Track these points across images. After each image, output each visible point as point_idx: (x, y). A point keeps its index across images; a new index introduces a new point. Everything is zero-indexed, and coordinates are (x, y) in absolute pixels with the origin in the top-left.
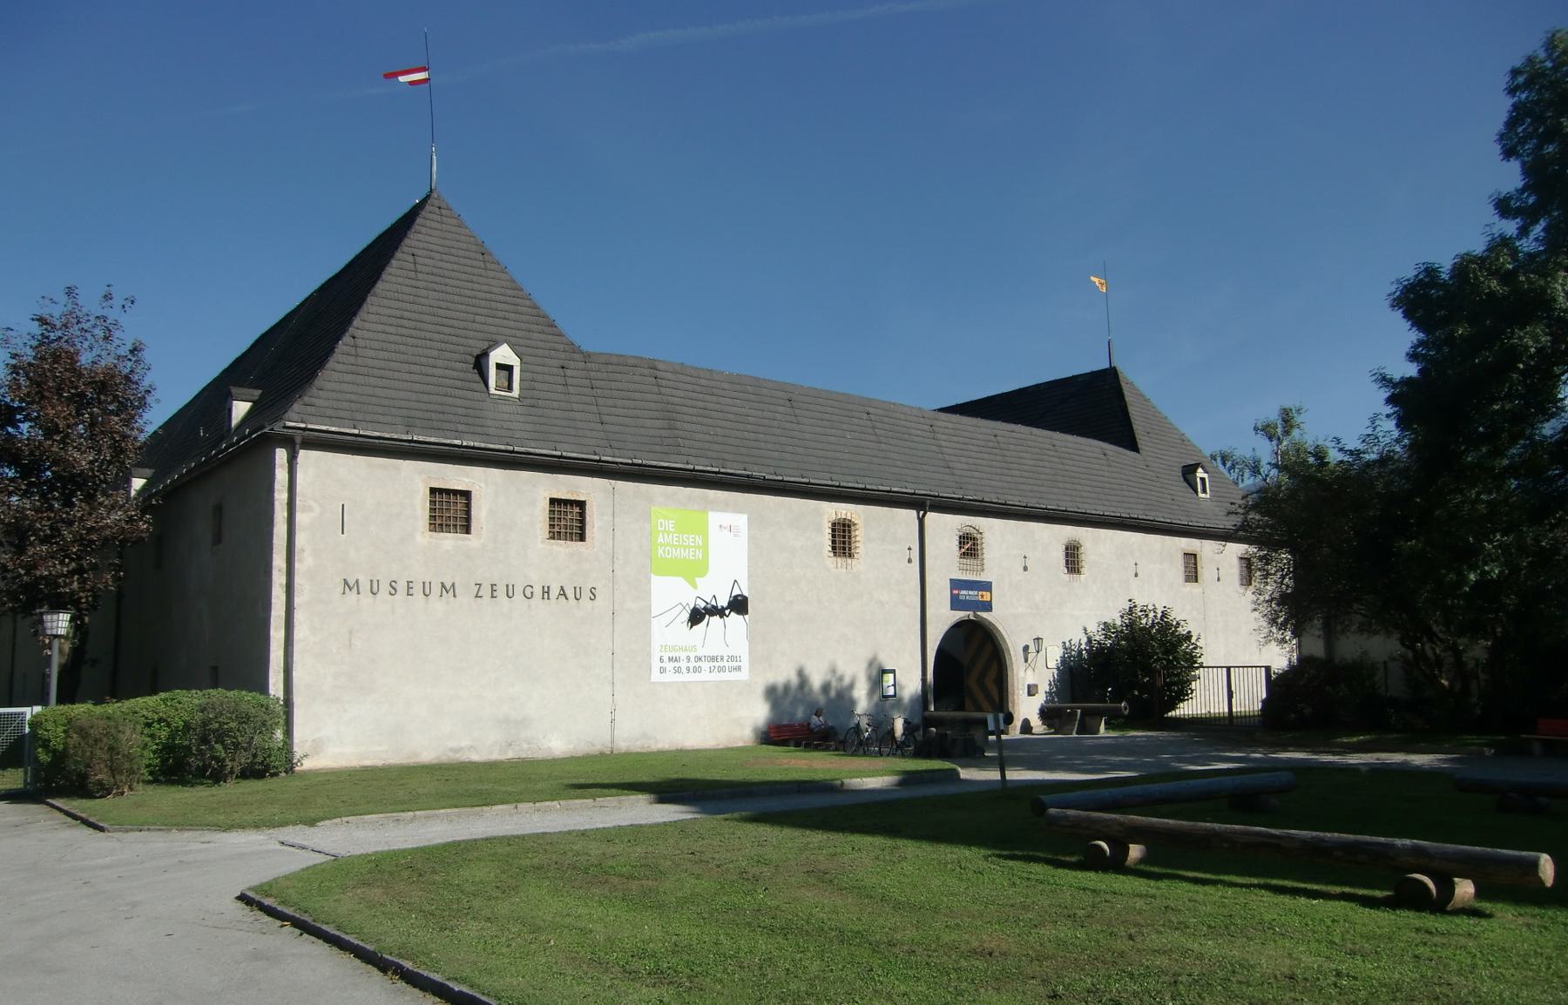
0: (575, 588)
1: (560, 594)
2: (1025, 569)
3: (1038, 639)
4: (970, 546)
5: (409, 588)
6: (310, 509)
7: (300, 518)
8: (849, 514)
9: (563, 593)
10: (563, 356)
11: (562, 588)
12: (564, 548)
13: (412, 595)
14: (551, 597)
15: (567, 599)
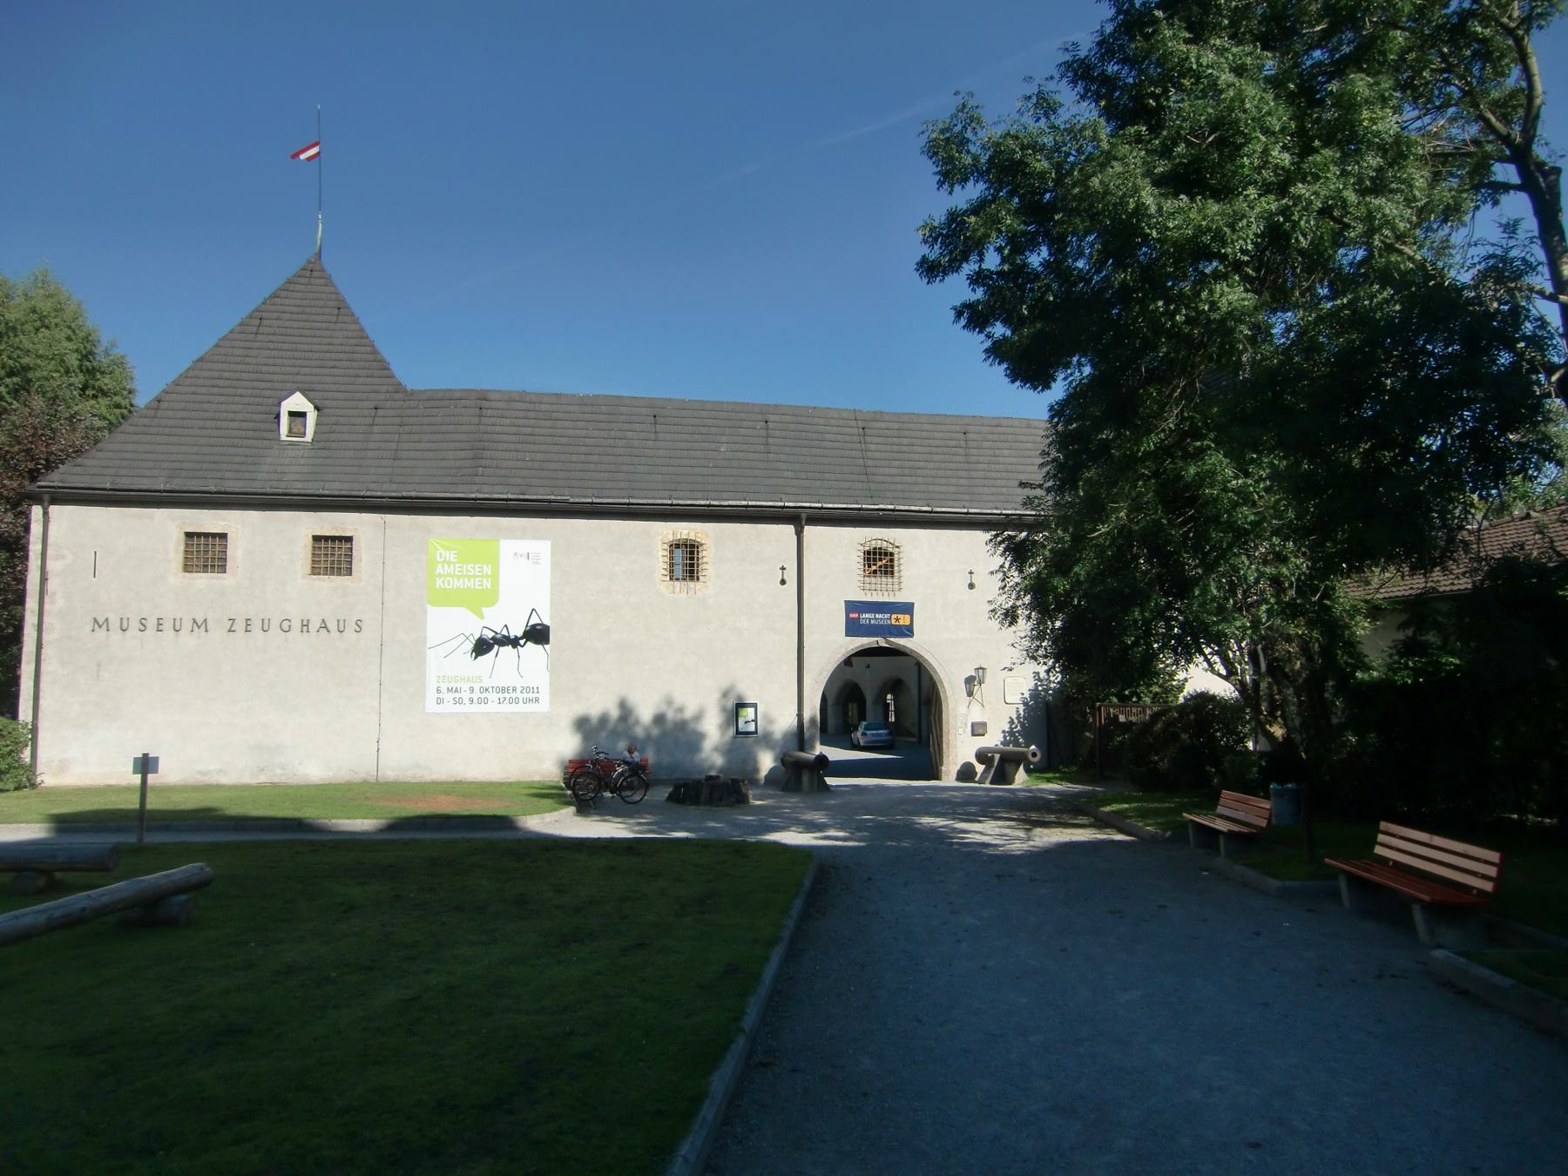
0: (338, 621)
7: (51, 565)
8: (693, 534)
9: (324, 626)
11: (323, 620)
12: (327, 583)
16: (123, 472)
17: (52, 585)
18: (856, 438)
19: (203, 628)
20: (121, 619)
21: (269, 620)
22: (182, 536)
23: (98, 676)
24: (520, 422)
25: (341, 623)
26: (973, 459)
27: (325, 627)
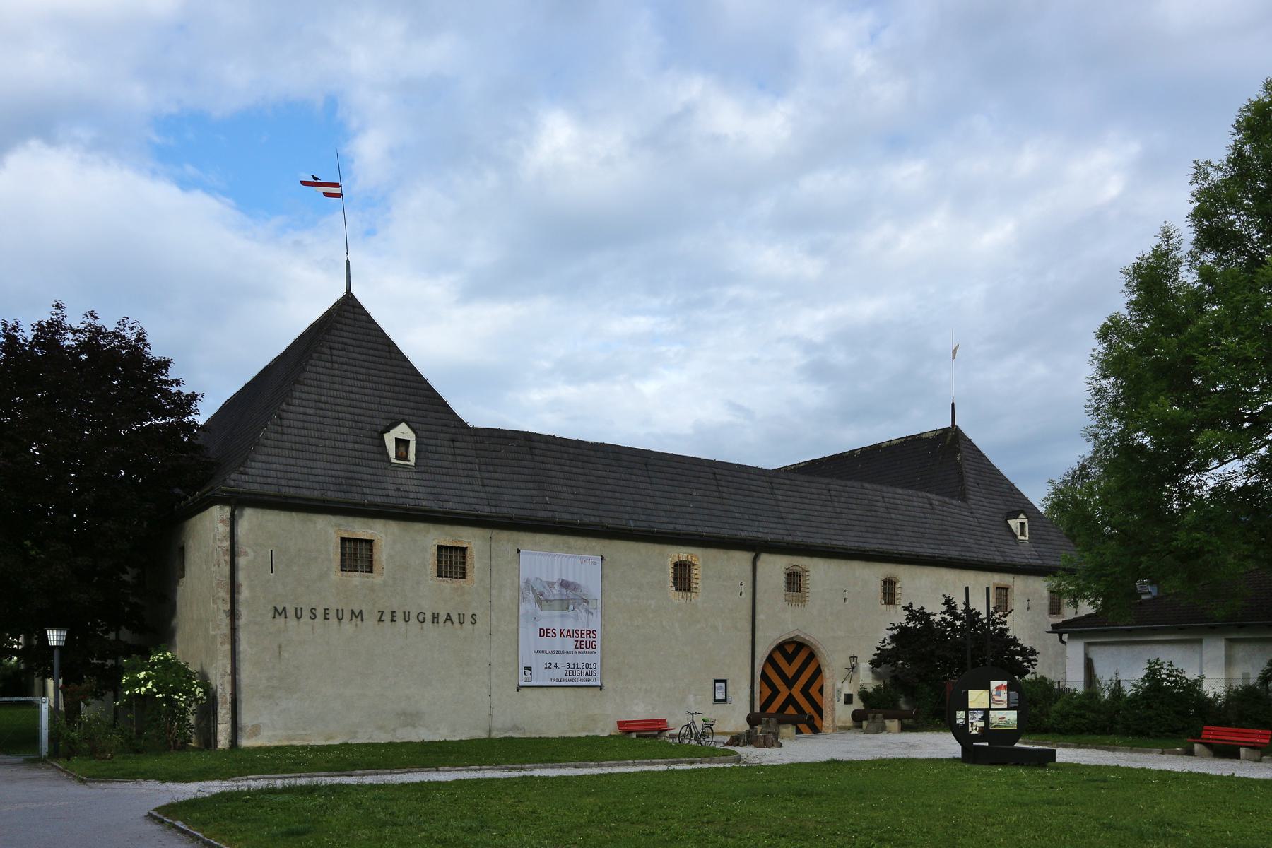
0: (459, 615)
1: (447, 619)
3: (854, 657)
4: (794, 581)
5: (326, 614)
6: (246, 554)
9: (449, 618)
10: (453, 430)
11: (449, 615)
12: (448, 584)
13: (328, 619)
14: (439, 621)
15: (453, 623)
19: (359, 618)
20: (296, 609)
21: (464, 615)
25: (462, 616)
26: (838, 510)
27: (451, 619)
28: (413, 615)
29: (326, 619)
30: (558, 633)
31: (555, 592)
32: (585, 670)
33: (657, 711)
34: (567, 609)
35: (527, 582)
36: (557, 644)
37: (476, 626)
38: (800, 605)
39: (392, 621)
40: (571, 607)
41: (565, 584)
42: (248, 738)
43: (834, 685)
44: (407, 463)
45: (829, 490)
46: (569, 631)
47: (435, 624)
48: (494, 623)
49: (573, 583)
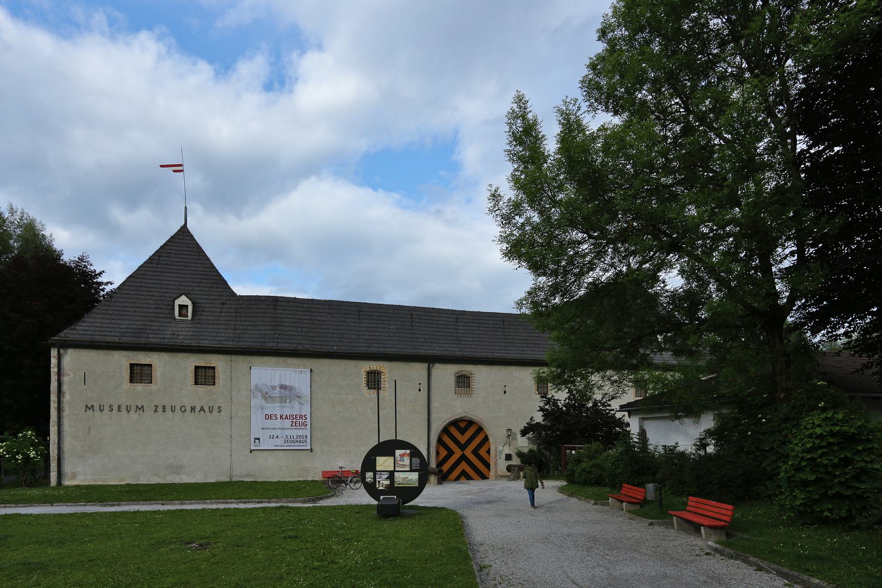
0: (210, 407)
1: (201, 410)
2: (505, 392)
4: (463, 382)
5: (119, 408)
6: (69, 375)
8: (378, 367)
9: (202, 409)
11: (202, 407)
14: (196, 411)
15: (205, 412)
16: (97, 333)
17: (65, 388)
18: (453, 323)
20: (100, 405)
22: (129, 366)
23: (89, 433)
24: (294, 312)
25: (211, 408)
26: (507, 334)
27: (203, 410)
28: (178, 408)
29: (119, 411)
30: (279, 417)
31: (276, 392)
32: (299, 439)
33: (354, 465)
34: (286, 402)
35: (256, 386)
36: (278, 423)
37: (221, 413)
38: (467, 396)
39: (164, 411)
40: (288, 401)
41: (283, 387)
42: (69, 480)
43: (496, 448)
44: (187, 318)
45: (503, 321)
46: (286, 415)
47: (193, 413)
48: (234, 412)
49: (290, 386)
